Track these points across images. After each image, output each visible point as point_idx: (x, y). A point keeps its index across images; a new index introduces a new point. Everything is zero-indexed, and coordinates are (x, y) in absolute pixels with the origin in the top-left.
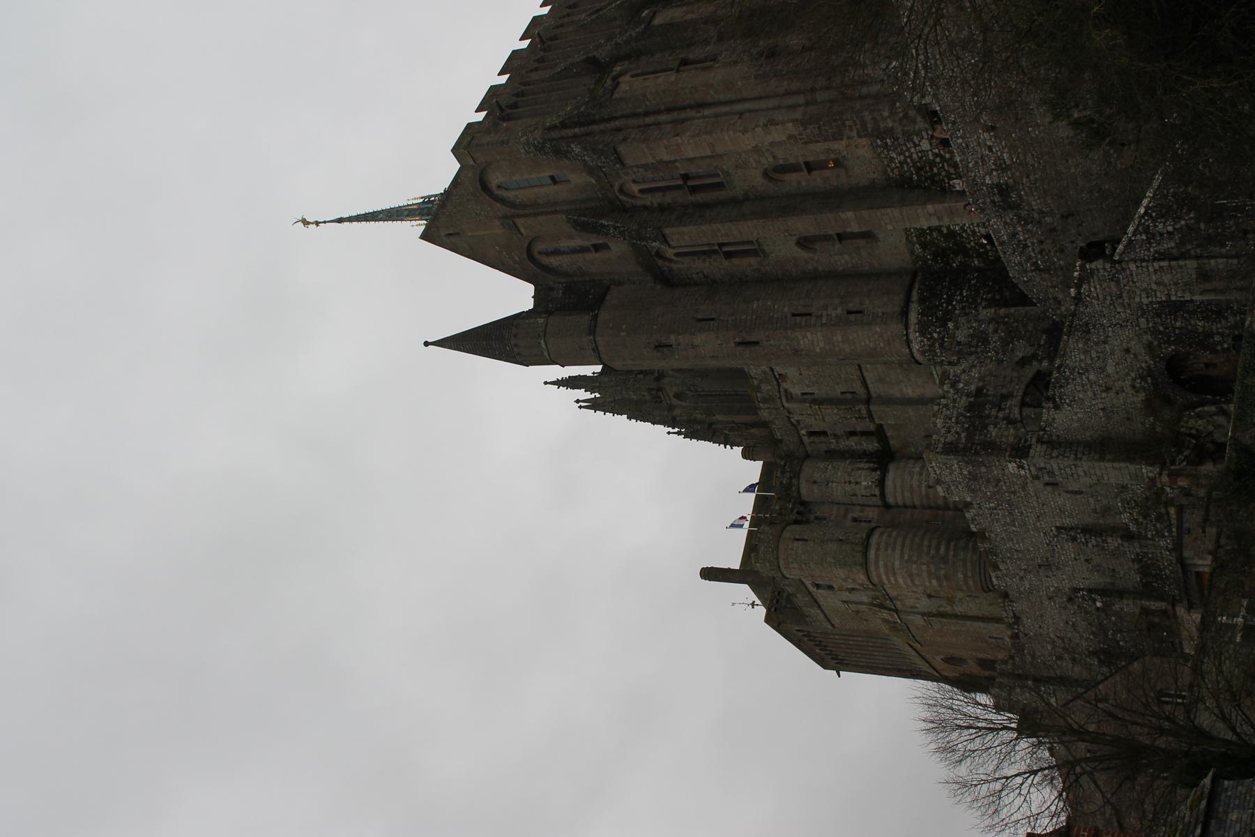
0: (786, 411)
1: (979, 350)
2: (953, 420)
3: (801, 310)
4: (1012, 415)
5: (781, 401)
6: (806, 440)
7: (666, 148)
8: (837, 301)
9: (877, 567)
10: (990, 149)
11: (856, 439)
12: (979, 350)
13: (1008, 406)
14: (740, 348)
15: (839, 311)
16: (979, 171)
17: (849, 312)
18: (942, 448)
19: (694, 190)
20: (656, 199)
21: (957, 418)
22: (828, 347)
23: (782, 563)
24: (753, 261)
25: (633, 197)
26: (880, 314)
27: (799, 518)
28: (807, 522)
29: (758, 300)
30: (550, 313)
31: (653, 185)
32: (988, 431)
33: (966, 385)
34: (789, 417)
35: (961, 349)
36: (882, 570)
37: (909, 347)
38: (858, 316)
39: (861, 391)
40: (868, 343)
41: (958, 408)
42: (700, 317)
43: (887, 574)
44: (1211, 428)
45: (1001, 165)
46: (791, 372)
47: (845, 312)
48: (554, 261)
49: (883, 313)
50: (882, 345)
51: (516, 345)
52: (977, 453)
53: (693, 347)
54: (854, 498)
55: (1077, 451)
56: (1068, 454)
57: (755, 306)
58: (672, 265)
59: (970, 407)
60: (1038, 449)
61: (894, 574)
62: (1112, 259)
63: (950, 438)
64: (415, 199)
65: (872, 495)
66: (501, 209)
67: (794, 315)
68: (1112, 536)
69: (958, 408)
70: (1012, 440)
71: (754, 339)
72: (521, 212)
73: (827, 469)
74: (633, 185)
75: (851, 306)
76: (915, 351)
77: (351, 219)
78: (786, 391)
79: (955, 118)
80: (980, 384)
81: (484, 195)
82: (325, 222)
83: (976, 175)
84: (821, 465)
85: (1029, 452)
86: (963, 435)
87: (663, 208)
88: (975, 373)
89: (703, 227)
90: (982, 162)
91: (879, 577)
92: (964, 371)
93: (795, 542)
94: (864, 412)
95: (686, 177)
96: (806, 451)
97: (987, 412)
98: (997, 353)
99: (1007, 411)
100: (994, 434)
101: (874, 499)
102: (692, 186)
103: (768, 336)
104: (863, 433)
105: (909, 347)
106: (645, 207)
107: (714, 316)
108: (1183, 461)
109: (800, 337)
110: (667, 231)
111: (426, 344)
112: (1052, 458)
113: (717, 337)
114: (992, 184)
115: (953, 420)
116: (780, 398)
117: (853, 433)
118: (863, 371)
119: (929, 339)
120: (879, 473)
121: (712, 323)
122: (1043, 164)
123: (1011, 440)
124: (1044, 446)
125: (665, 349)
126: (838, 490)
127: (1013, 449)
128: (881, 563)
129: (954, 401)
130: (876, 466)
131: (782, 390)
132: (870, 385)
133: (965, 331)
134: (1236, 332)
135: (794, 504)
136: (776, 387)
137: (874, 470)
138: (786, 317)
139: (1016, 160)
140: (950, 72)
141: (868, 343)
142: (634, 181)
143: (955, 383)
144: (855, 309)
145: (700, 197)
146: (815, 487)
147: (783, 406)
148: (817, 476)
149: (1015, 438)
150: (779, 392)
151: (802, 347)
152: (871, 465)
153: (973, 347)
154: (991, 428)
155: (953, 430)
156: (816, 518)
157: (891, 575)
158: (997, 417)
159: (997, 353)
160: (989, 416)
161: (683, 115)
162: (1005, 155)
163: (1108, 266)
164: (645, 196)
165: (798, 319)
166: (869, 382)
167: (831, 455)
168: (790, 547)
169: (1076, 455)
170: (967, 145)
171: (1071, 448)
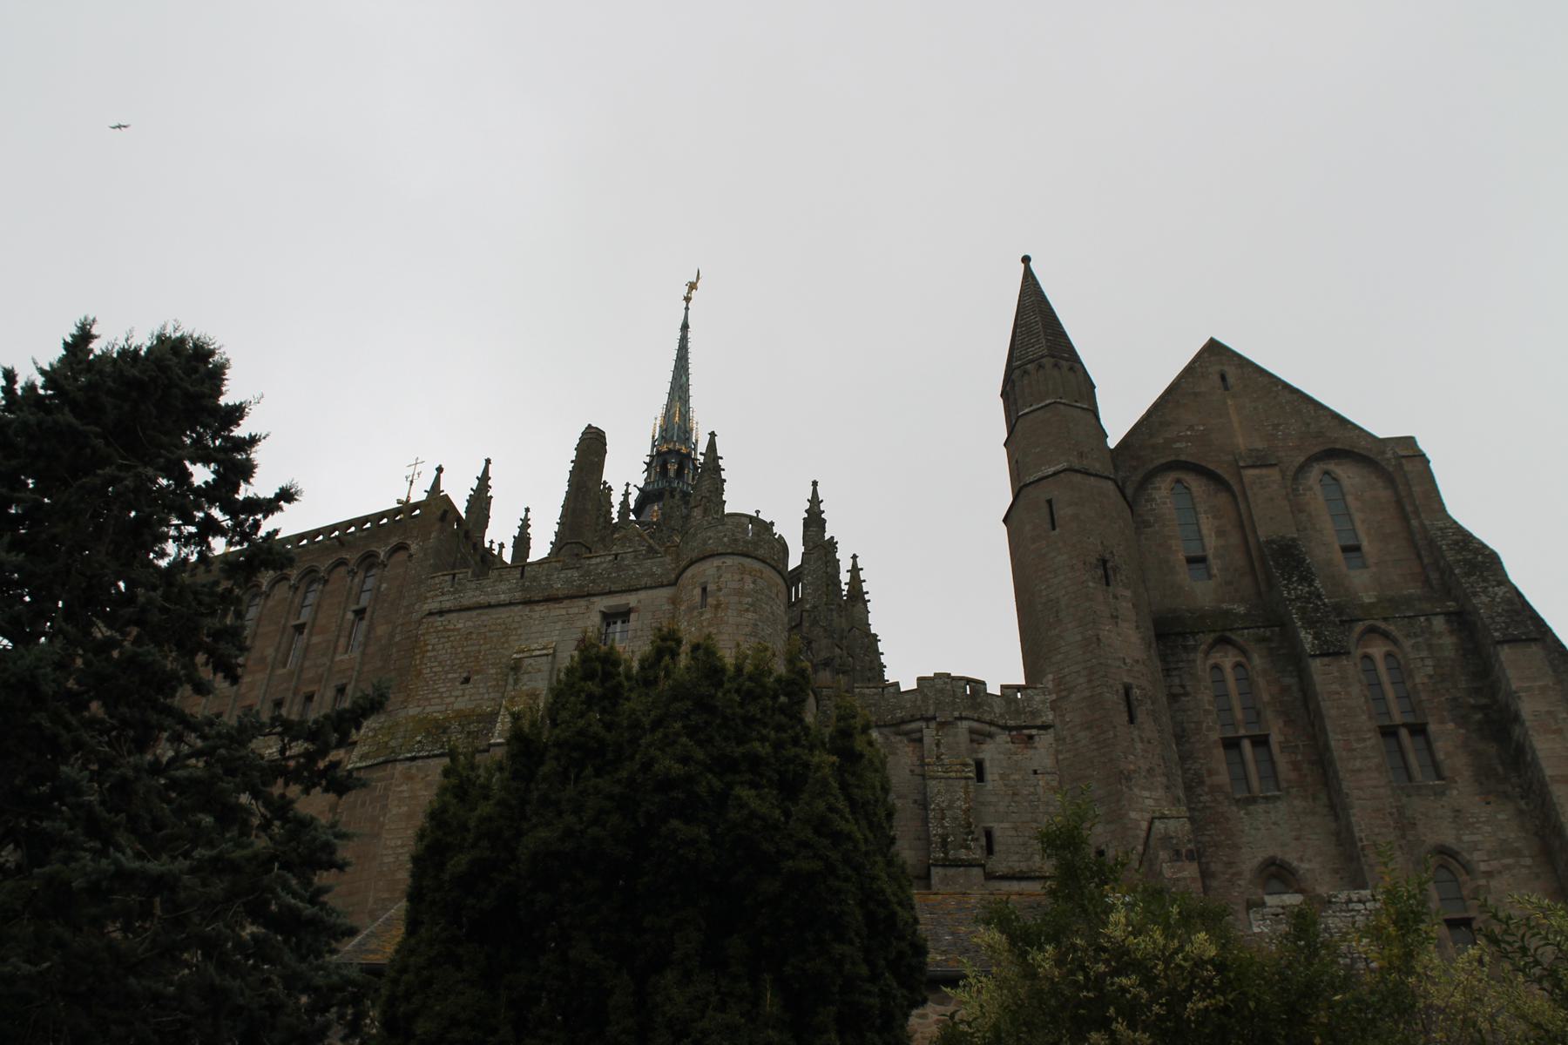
0: (950, 719)
5: (973, 719)
23: (757, 565)
64: (697, 435)
77: (684, 341)
78: (991, 736)
81: (1322, 448)
82: (687, 309)
103: (1149, 742)
113: (1137, 661)
116: (978, 720)
131: (993, 729)
136: (1001, 722)
147: (961, 718)
150: (991, 723)
151: (1136, 790)
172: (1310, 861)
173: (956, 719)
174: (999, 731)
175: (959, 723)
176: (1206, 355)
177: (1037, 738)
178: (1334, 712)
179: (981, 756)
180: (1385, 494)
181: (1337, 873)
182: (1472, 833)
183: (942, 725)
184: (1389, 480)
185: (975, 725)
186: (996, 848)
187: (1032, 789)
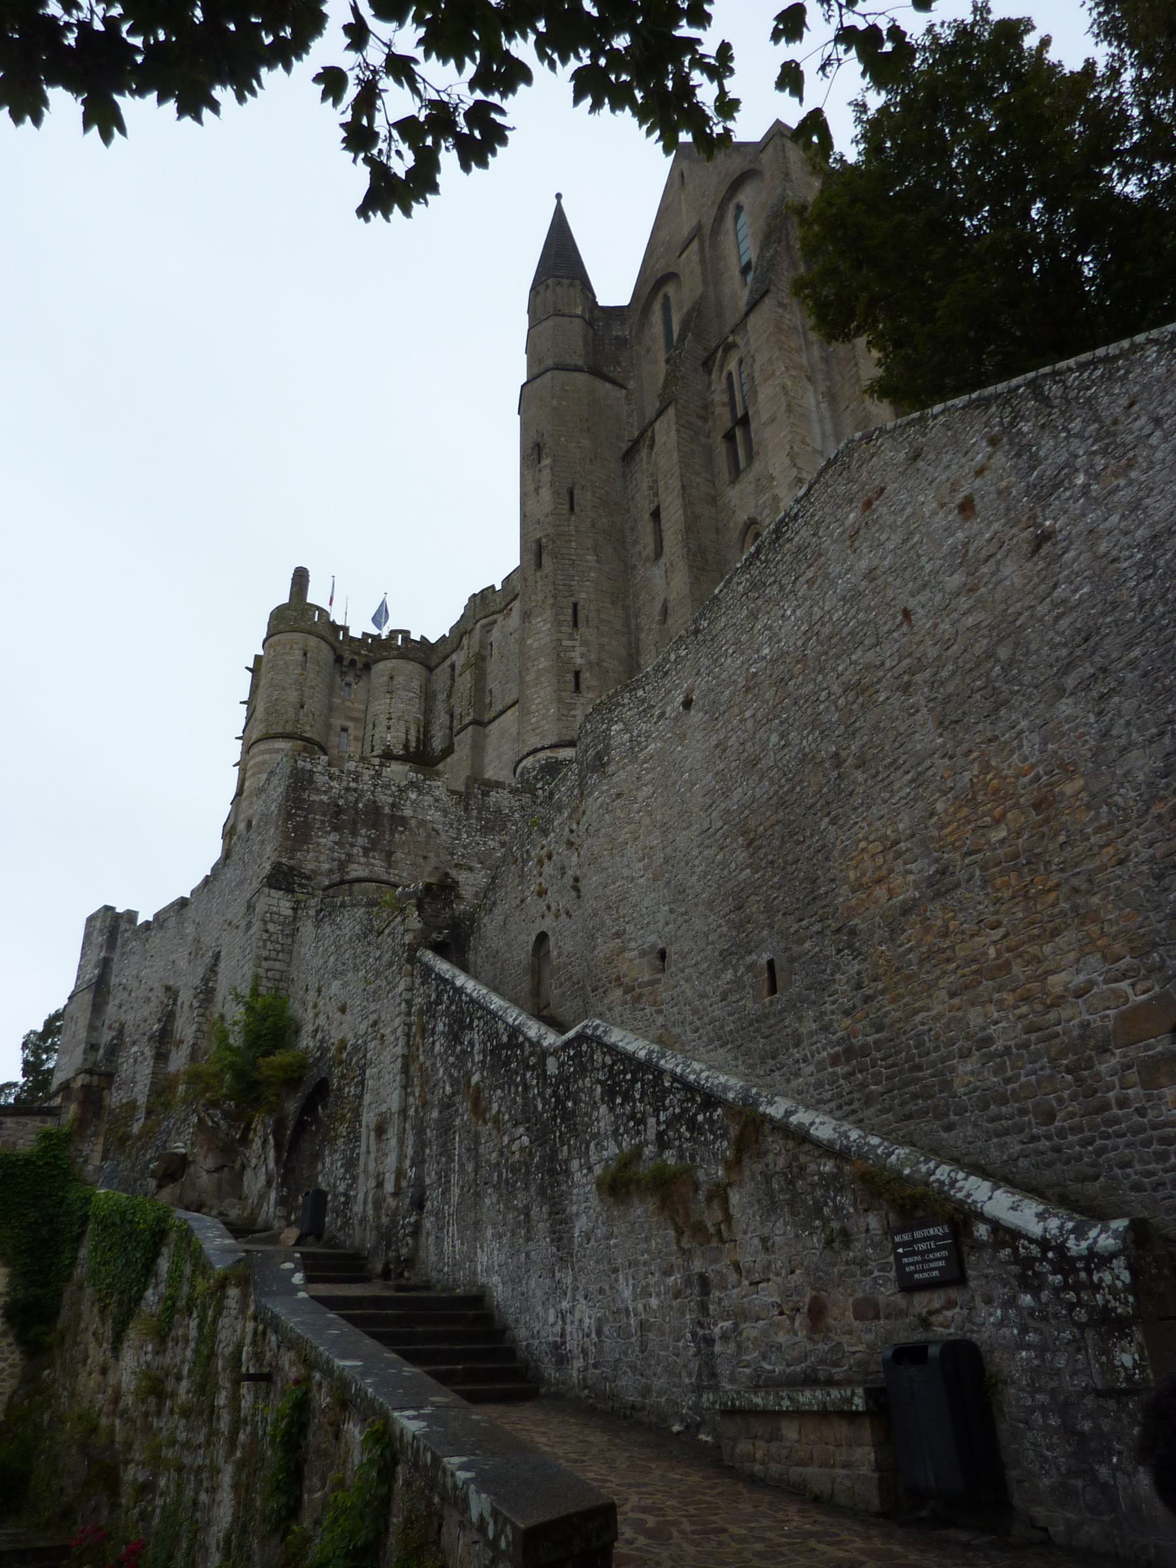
0: (471, 626)
1: (473, 821)
2: (353, 785)
3: (581, 615)
4: (355, 866)
6: (448, 662)
7: (770, 361)
8: (593, 657)
9: (263, 752)
10: (663, 713)
11: (448, 723)
12: (473, 821)
13: (372, 861)
14: (534, 546)
15: (579, 661)
16: (630, 709)
17: (577, 674)
18: (303, 769)
19: (730, 437)
20: (719, 396)
21: (355, 790)
22: (532, 653)
24: (651, 547)
25: (722, 367)
26: (572, 713)
27: (345, 663)
28: (343, 674)
29: (597, 561)
30: (590, 324)
31: (736, 386)
32: (329, 833)
33: (412, 803)
34: (466, 633)
35: (476, 797)
36: (259, 759)
37: (528, 755)
38: (571, 686)
39: (493, 714)
40: (537, 701)
41: (373, 792)
42: (576, 492)
43: (256, 765)
44: (254, 1162)
45: (639, 743)
46: (515, 619)
47: (578, 669)
48: (657, 316)
49: (574, 716)
50: (533, 720)
51: (548, 286)
52: (289, 816)
53: (537, 489)
54: (371, 726)
55: (275, 960)
56: (269, 946)
57: (589, 557)
58: (645, 451)
59: (374, 809)
60: (282, 903)
61: (253, 775)
62: (419, 945)
63: (320, 779)
65: (373, 747)
66: (708, 221)
67: (575, 605)
68: (198, 1030)
69: (373, 792)
70: (310, 867)
71: (546, 559)
72: (707, 244)
73: (409, 691)
74: (737, 359)
75: (585, 675)
76: (524, 763)
78: (495, 622)
79: (704, 629)
80: (413, 822)
83: (624, 705)
84: (415, 684)
85: (280, 889)
86: (325, 798)
87: (706, 409)
88: (433, 815)
89: (676, 454)
90: (644, 711)
91: (253, 757)
92: (437, 800)
93: (302, 652)
94: (467, 720)
95: (744, 422)
96: (436, 667)
97: (363, 831)
98: (465, 847)
99: (362, 860)
100: (323, 841)
101: (369, 750)
102: (734, 436)
104: (451, 728)
105: (528, 755)
106: (710, 384)
107: (577, 509)
108: (213, 1122)
109: (544, 617)
110: (671, 411)
111: (559, 196)
112: (265, 923)
114: (611, 737)
115: (353, 785)
117: (452, 716)
118: (513, 709)
119: (535, 777)
120: (401, 752)
121: (567, 507)
122: (637, 817)
123: (310, 866)
124: (290, 912)
125: (535, 456)
126: (380, 706)
127: (291, 868)
128: (267, 757)
129: (387, 786)
130: (412, 750)
131: (495, 616)
132: (496, 722)
133: (506, 803)
134: (329, 1198)
135: (365, 656)
137: (406, 746)
138: (572, 595)
139: (645, 769)
140: (772, 579)
141: (537, 701)
142: (741, 362)
143: (418, 788)
144: (581, 680)
145: (721, 448)
146: (385, 678)
148: (399, 679)
149: (313, 871)
150: (493, 613)
151: (533, 621)
152: (414, 744)
153: (479, 813)
154: (334, 837)
155: (334, 784)
156: (348, 685)
157: (255, 769)
158: (352, 845)
159: (465, 847)
160: (354, 833)
161: (819, 376)
162: (653, 746)
163: (408, 938)
164: (724, 380)
165: (570, 611)
166: (502, 718)
167: (428, 696)
168: (295, 646)
169: (266, 959)
170: (666, 674)
171: (282, 951)
185: (484, 621)
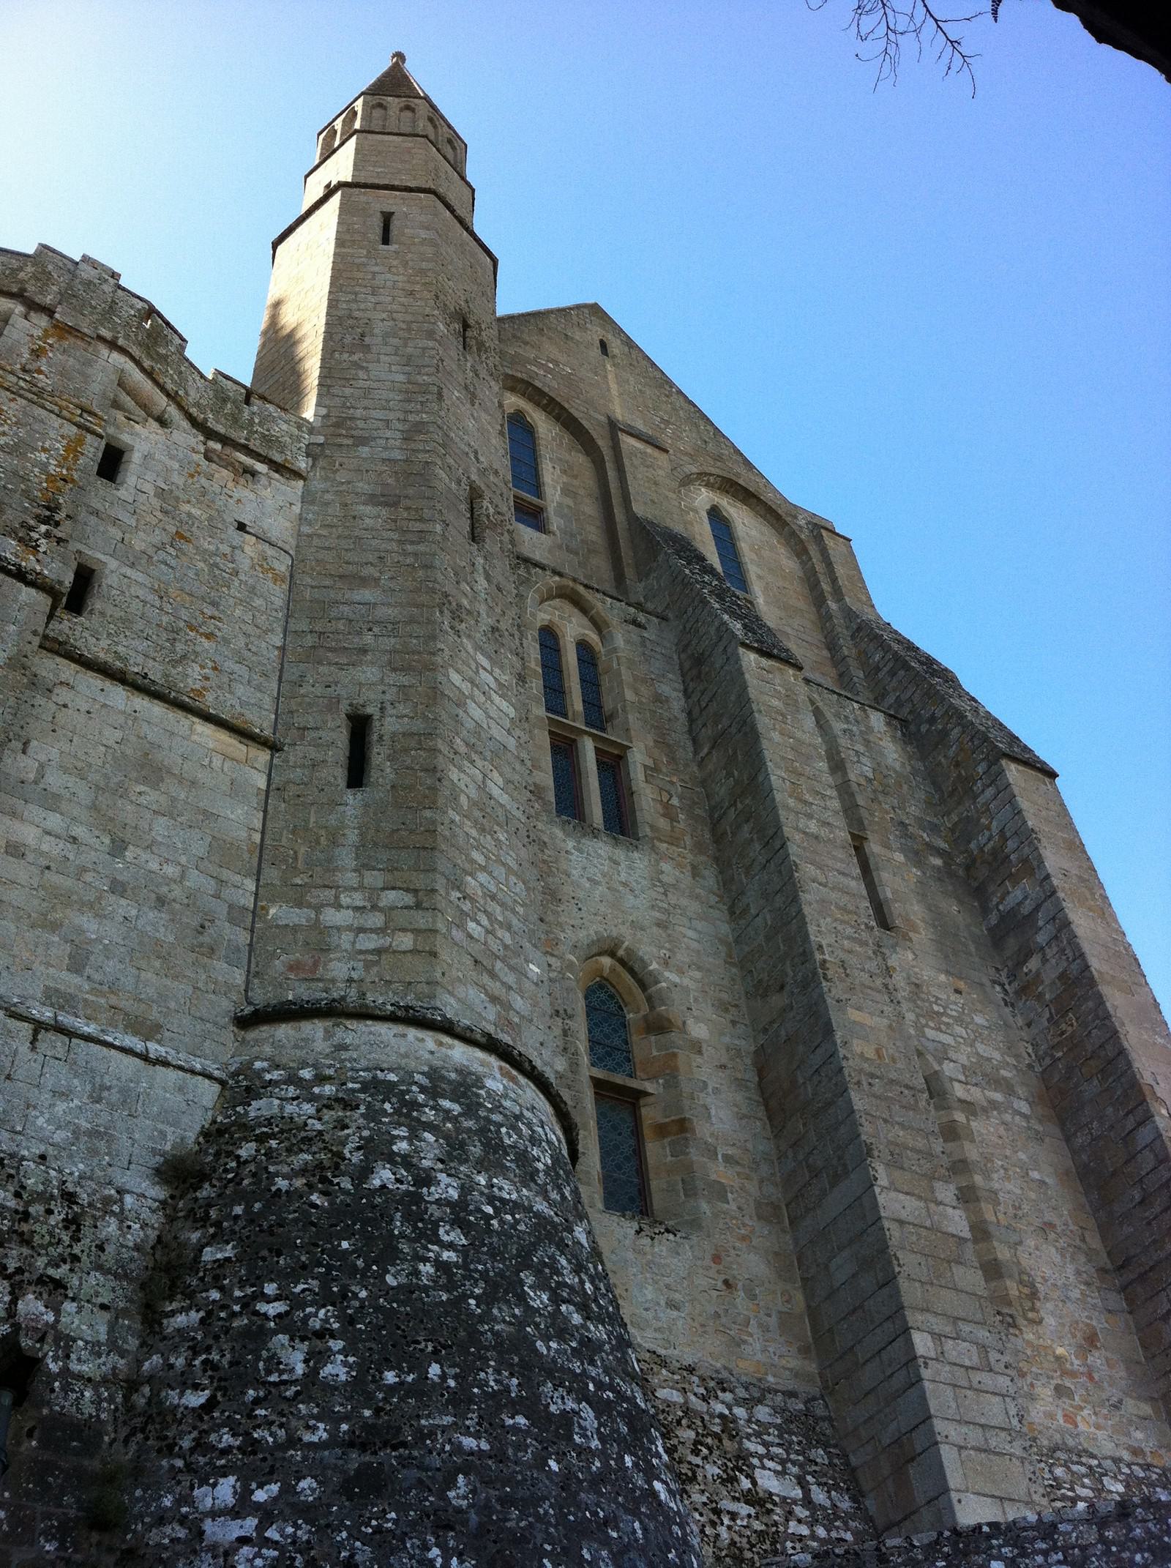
5: (138, 363)
131: (173, 411)
147: (113, 345)
172: (681, 972)
173: (101, 338)
174: (185, 424)
175: (104, 351)
176: (586, 311)
177: (264, 480)
178: (776, 736)
179: (126, 438)
180: (789, 564)
181: (727, 1010)
182: (939, 1029)
183: (65, 331)
184: (800, 551)
186: (96, 603)
187: (227, 550)
